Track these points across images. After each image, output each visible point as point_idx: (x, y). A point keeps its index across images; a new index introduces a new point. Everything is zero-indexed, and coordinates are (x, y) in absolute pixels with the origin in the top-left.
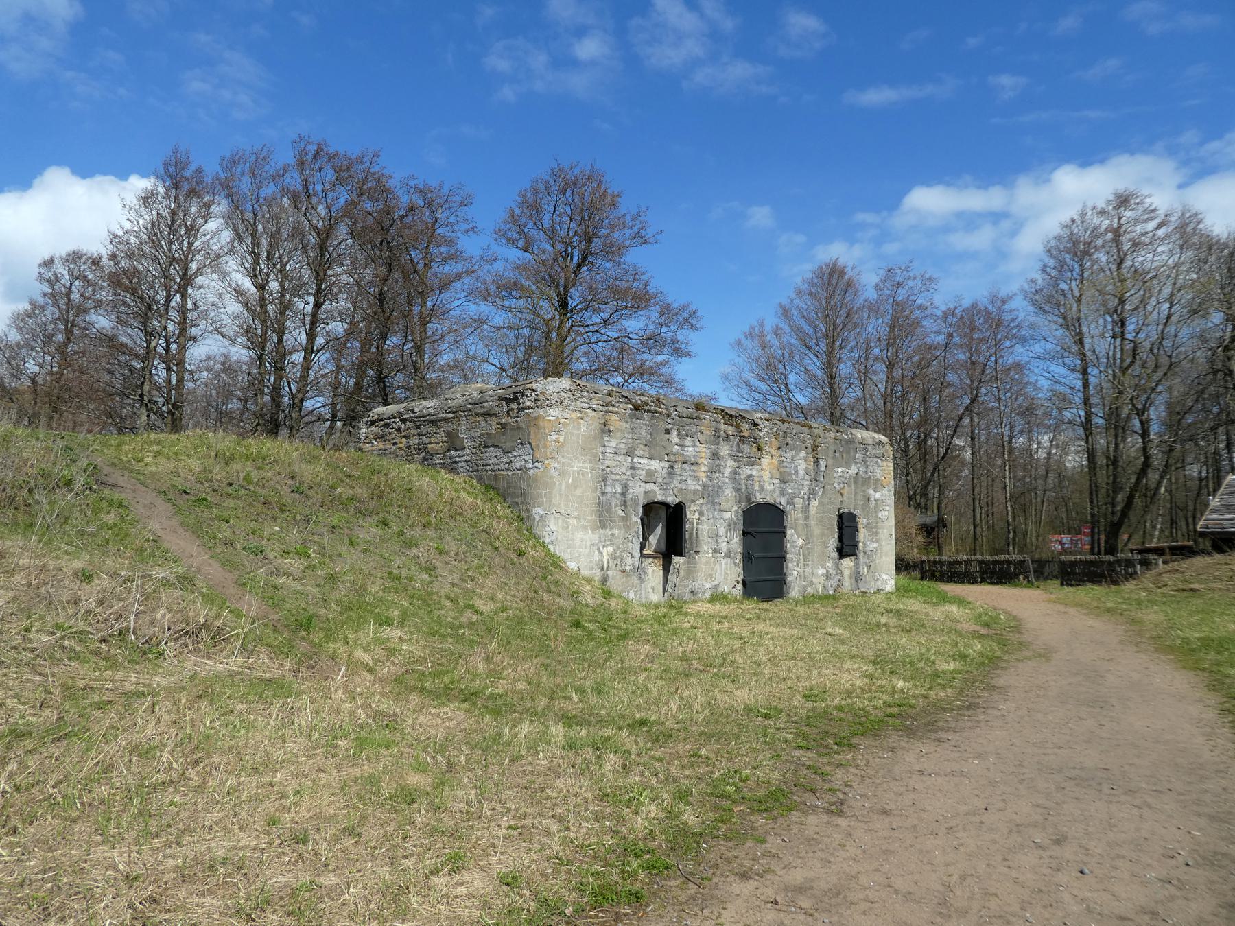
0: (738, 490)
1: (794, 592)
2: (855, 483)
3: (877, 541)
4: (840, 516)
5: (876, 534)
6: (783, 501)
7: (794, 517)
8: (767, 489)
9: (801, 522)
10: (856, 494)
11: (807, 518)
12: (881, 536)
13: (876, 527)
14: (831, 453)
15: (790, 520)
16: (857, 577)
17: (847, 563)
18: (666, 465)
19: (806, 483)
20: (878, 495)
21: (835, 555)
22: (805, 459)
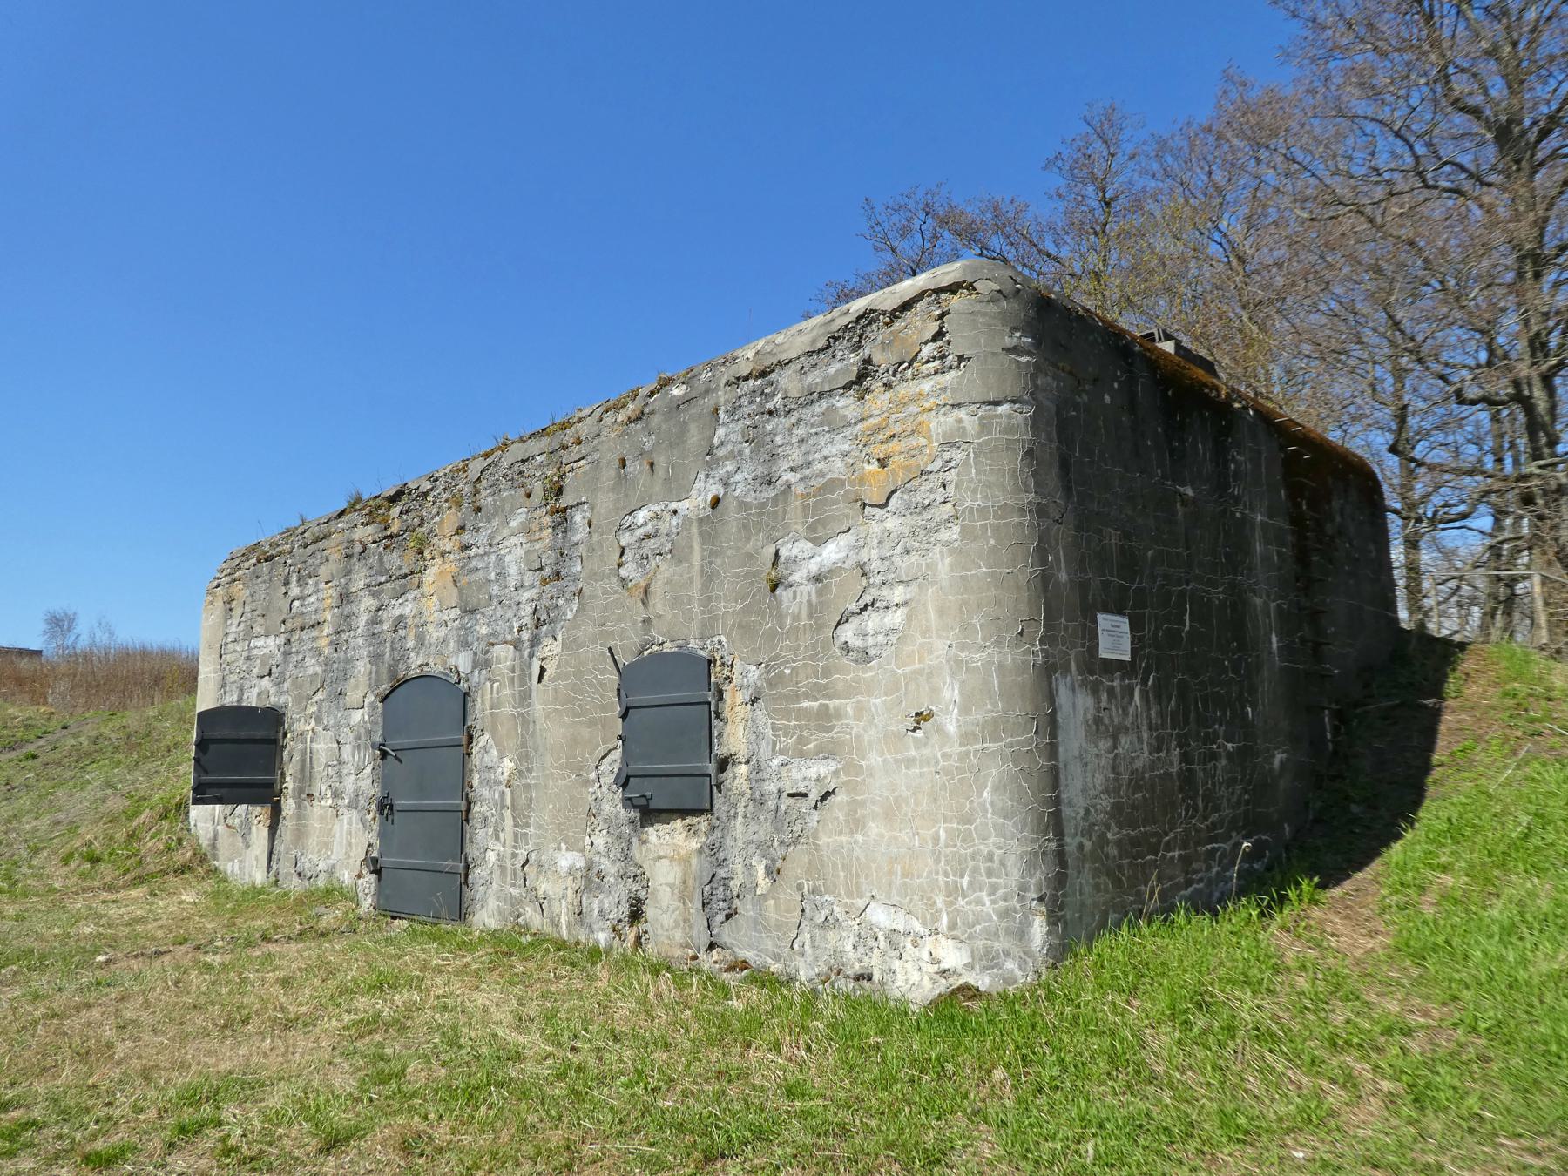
0: (376, 658)
1: (486, 916)
2: (708, 537)
3: (825, 752)
4: (629, 678)
5: (824, 719)
6: (463, 661)
7: (493, 700)
8: (438, 645)
9: (507, 710)
10: (708, 577)
11: (525, 697)
12: (851, 726)
13: (825, 692)
14: (609, 473)
15: (480, 709)
16: (716, 899)
17: (671, 847)
18: (282, 640)
19: (526, 595)
20: (832, 552)
21: (612, 804)
22: (526, 530)
